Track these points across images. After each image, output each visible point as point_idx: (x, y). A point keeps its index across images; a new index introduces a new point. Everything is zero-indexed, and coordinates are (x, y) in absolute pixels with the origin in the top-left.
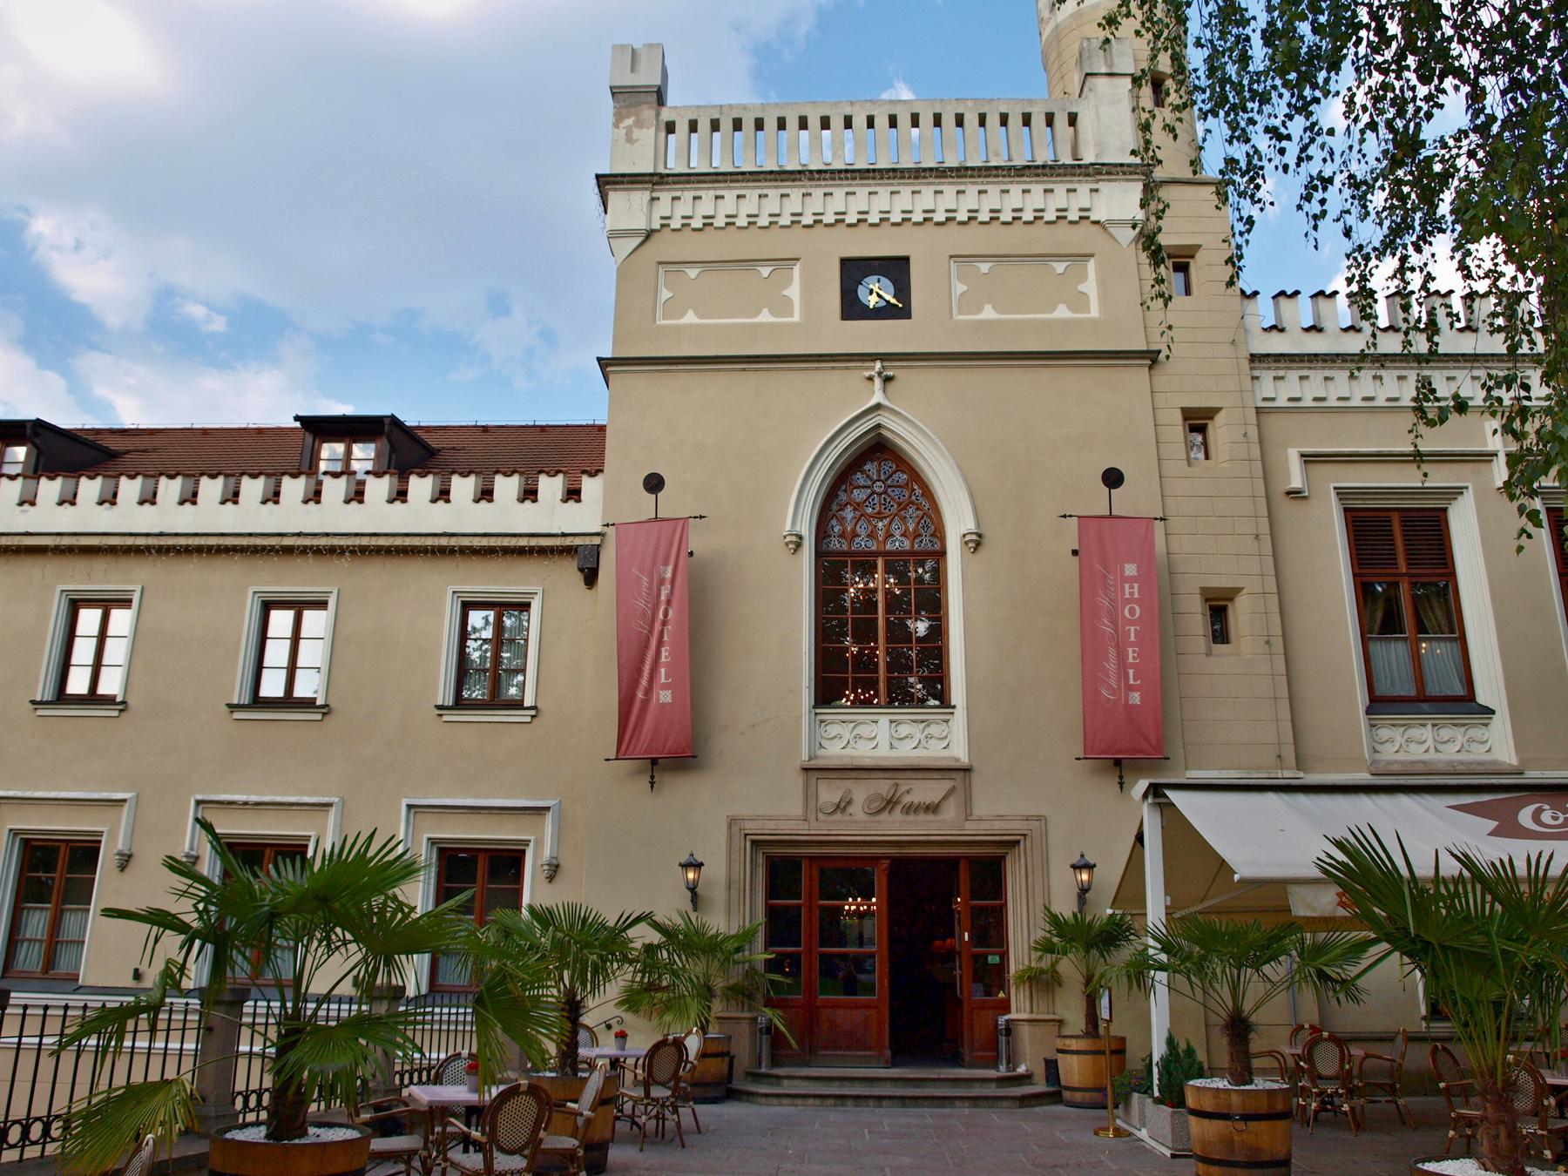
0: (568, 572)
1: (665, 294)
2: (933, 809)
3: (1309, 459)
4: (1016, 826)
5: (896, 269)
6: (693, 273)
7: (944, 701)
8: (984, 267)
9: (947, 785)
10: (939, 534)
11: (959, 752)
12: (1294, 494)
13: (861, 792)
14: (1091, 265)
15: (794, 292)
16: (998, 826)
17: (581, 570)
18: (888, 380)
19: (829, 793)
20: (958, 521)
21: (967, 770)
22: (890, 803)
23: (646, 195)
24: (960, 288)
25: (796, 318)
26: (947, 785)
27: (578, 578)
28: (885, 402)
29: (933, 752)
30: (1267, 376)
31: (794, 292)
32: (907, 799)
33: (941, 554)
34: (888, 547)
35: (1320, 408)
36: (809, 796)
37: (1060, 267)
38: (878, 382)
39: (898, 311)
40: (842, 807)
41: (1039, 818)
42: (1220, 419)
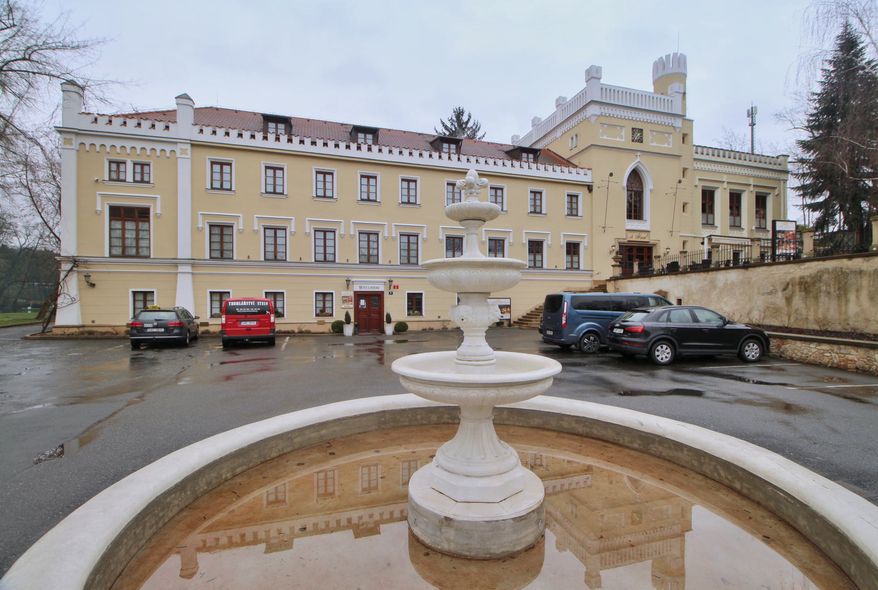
0: (586, 189)
1: (601, 131)
2: (645, 238)
3: (700, 180)
5: (641, 131)
6: (606, 126)
8: (655, 133)
12: (696, 186)
13: (635, 234)
14: (671, 135)
15: (623, 133)
16: (654, 242)
17: (589, 189)
19: (630, 234)
22: (639, 237)
23: (599, 106)
24: (650, 137)
27: (588, 191)
29: (643, 228)
30: (695, 163)
31: (623, 133)
32: (642, 236)
35: (701, 170)
36: (627, 235)
37: (666, 135)
39: (640, 141)
40: (632, 237)
42: (688, 170)
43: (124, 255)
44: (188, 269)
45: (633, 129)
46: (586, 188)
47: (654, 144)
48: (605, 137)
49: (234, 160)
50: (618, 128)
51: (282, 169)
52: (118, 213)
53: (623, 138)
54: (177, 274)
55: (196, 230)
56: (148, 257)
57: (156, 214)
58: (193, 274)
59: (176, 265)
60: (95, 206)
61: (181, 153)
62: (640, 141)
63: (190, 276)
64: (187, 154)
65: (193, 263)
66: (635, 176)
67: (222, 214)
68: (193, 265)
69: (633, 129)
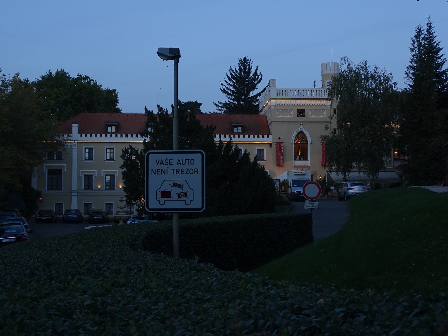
4: (314, 173)
7: (307, 160)
9: (308, 168)
10: (307, 141)
11: (309, 165)
15: (292, 113)
18: (302, 125)
20: (309, 141)
21: (310, 167)
24: (310, 113)
25: (292, 117)
26: (308, 168)
27: (270, 147)
28: (302, 128)
31: (292, 113)
33: (307, 144)
34: (302, 143)
38: (301, 125)
39: (303, 116)
41: (317, 172)
43: (52, 189)
44: (76, 194)
45: (298, 110)
46: (269, 145)
47: (313, 117)
48: (280, 116)
49: (94, 147)
50: (289, 110)
51: (113, 149)
52: (51, 172)
53: (292, 116)
54: (72, 196)
55: (79, 178)
56: (61, 189)
57: (64, 172)
58: (77, 196)
59: (71, 193)
60: (43, 170)
61: (74, 147)
62: (303, 116)
63: (76, 197)
64: (76, 147)
65: (78, 191)
66: (301, 135)
67: (88, 171)
68: (78, 192)
69: (298, 110)
